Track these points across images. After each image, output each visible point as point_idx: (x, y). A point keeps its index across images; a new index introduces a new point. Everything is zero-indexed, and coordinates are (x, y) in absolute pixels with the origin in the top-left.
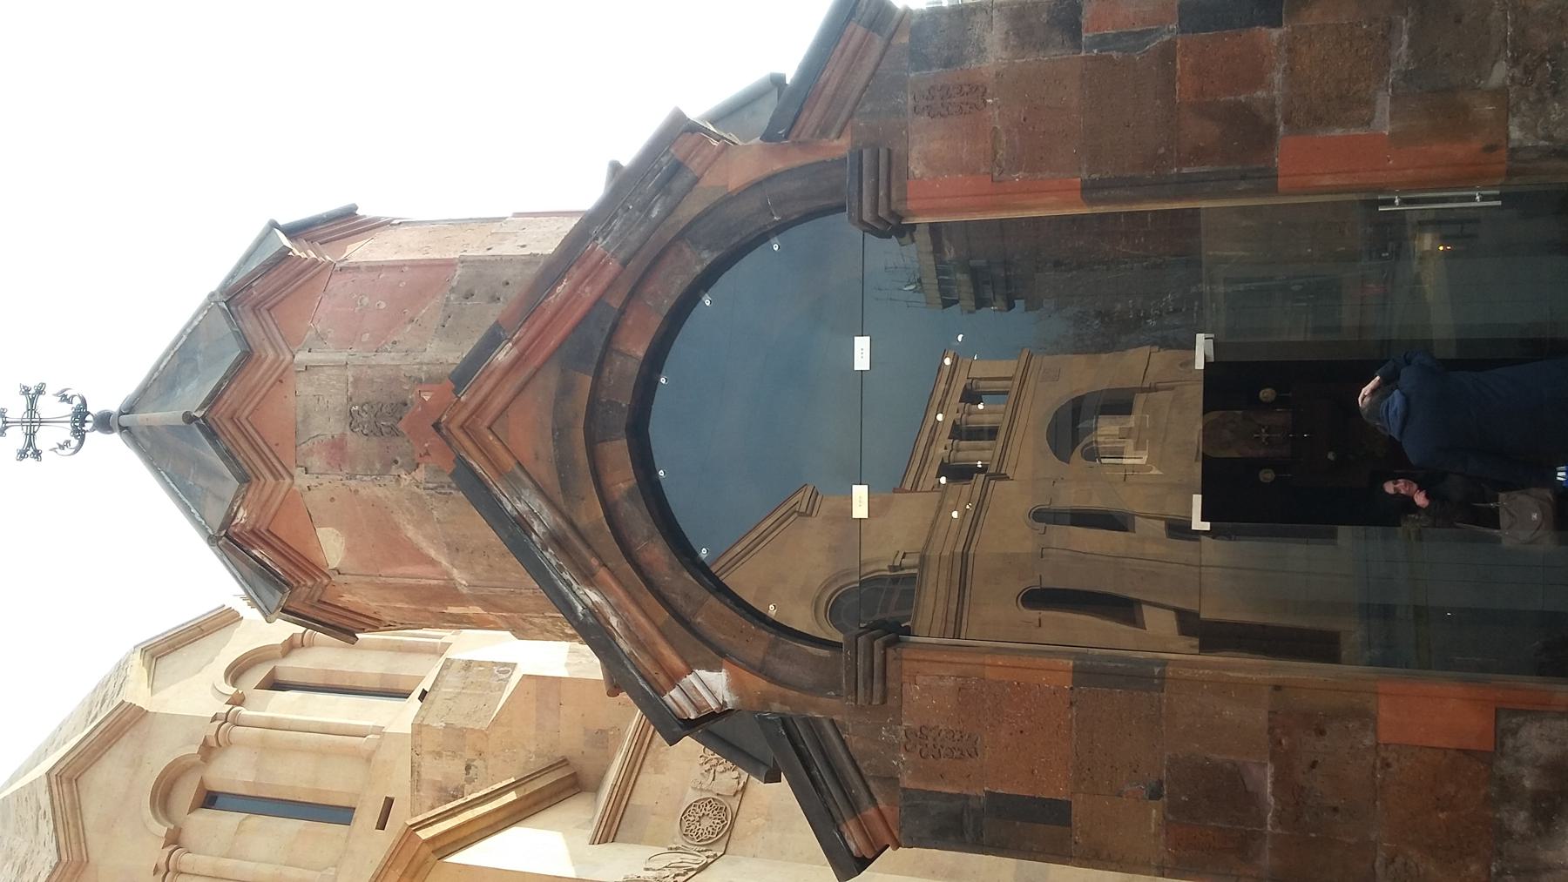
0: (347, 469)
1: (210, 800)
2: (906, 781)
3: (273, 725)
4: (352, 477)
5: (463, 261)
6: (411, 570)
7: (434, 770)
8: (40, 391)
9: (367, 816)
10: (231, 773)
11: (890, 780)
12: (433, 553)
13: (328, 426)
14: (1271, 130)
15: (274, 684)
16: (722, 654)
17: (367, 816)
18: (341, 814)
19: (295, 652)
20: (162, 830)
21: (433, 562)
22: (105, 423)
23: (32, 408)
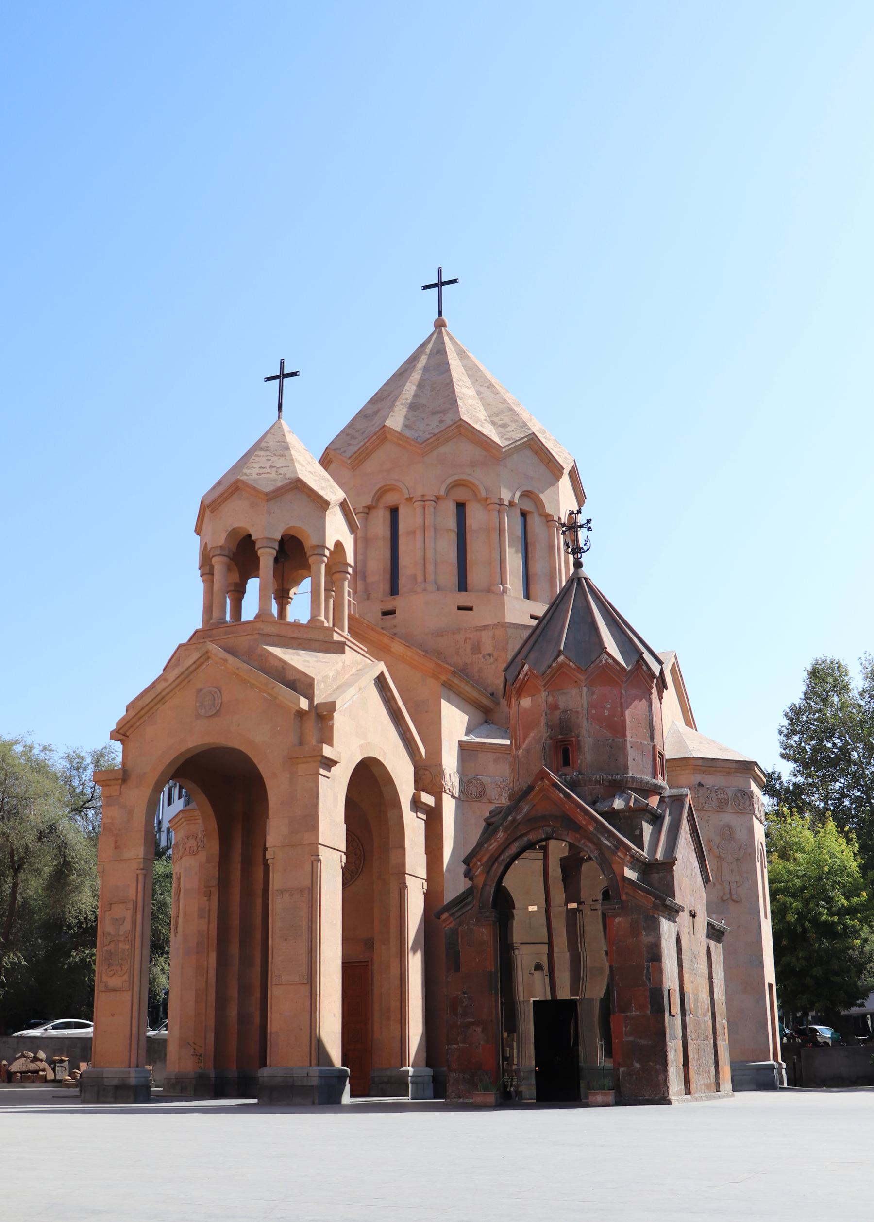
0: (548, 712)
1: (461, 507)
2: (460, 929)
3: (501, 531)
4: (546, 715)
5: (625, 741)
6: (521, 736)
7: (486, 638)
8: (589, 529)
9: (464, 599)
10: (476, 517)
11: (460, 925)
12: (526, 742)
13: (563, 701)
14: (624, 1012)
15: (524, 514)
16: (488, 873)
17: (464, 599)
18: (463, 585)
19: (544, 519)
20: (442, 493)
21: (524, 742)
22: (578, 565)
23: (582, 526)
